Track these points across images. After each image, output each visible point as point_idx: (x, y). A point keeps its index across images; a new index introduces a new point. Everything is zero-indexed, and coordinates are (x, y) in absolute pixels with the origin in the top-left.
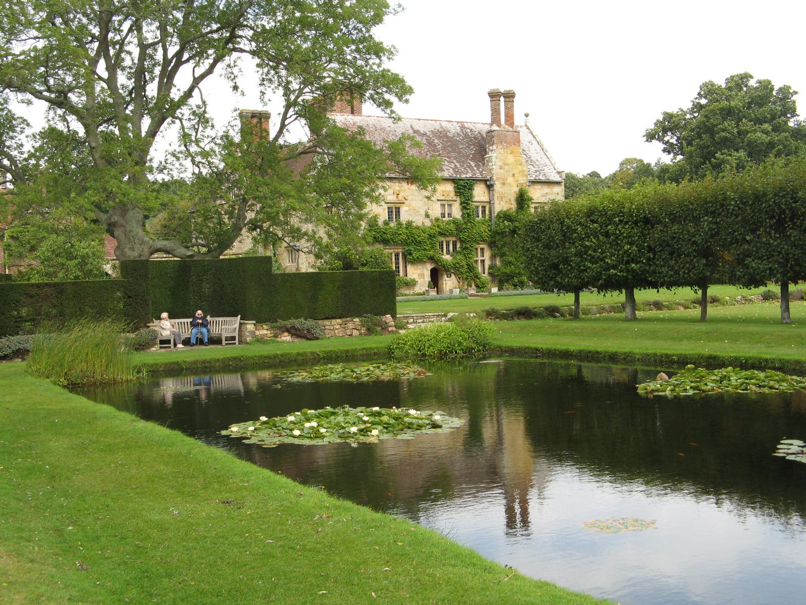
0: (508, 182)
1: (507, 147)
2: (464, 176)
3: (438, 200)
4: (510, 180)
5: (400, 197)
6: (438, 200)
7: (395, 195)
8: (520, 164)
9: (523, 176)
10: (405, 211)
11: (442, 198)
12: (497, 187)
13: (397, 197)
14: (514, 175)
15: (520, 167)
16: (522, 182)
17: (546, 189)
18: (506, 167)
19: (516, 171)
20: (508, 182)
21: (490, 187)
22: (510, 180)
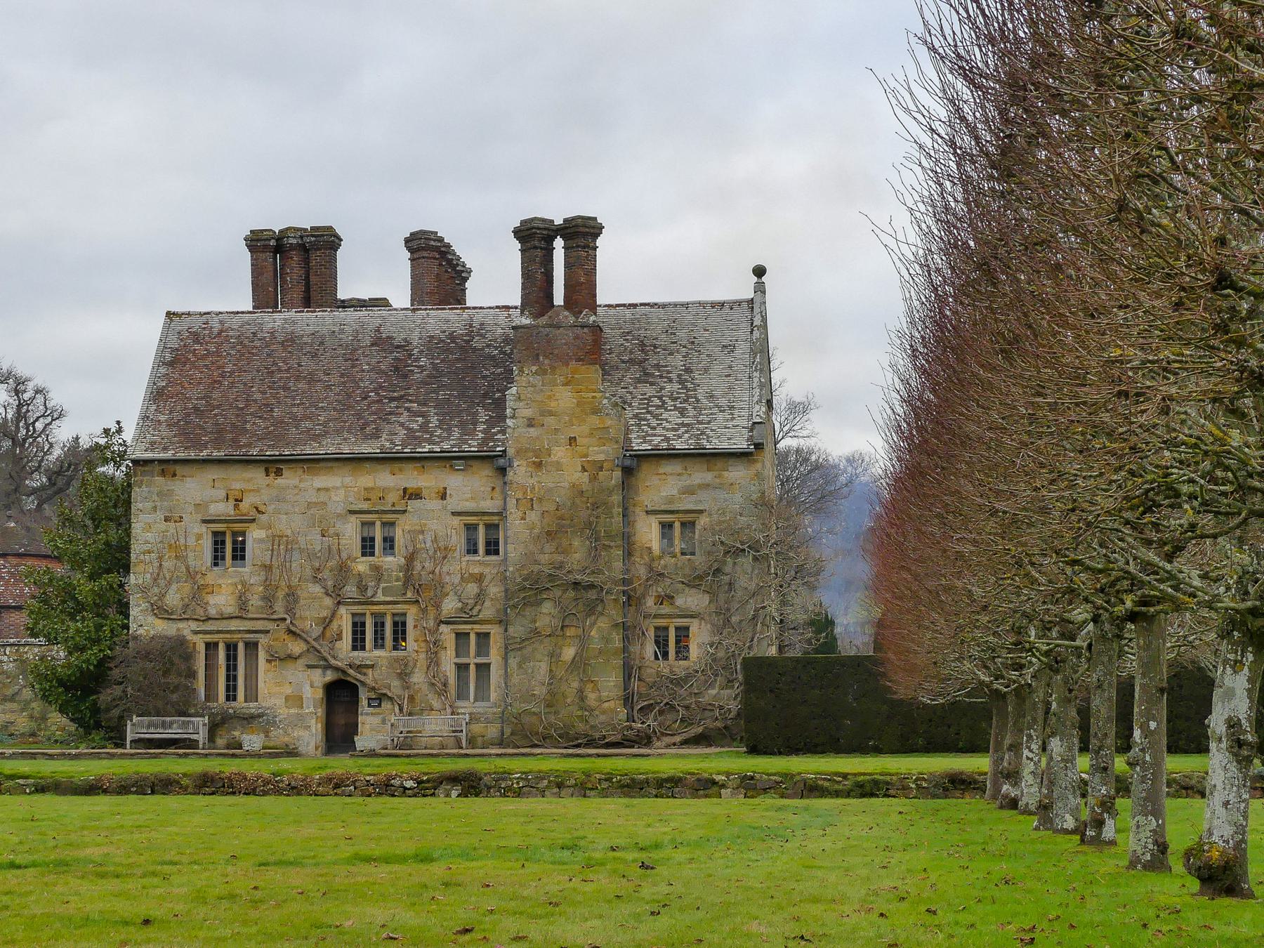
0: (554, 458)
1: (553, 368)
2: (427, 448)
3: (352, 512)
4: (560, 453)
5: (244, 506)
6: (352, 512)
7: (232, 502)
8: (596, 411)
9: (603, 441)
10: (254, 540)
11: (365, 506)
12: (520, 472)
13: (236, 506)
14: (572, 440)
15: (594, 420)
16: (601, 457)
17: (700, 475)
18: (550, 421)
19: (575, 431)
20: (554, 458)
21: (502, 471)
22: (560, 453)
